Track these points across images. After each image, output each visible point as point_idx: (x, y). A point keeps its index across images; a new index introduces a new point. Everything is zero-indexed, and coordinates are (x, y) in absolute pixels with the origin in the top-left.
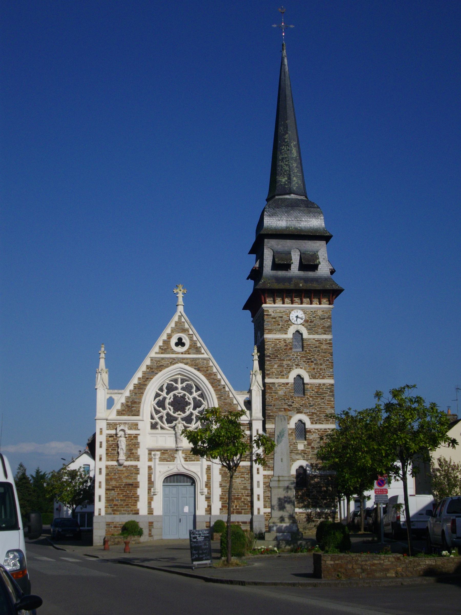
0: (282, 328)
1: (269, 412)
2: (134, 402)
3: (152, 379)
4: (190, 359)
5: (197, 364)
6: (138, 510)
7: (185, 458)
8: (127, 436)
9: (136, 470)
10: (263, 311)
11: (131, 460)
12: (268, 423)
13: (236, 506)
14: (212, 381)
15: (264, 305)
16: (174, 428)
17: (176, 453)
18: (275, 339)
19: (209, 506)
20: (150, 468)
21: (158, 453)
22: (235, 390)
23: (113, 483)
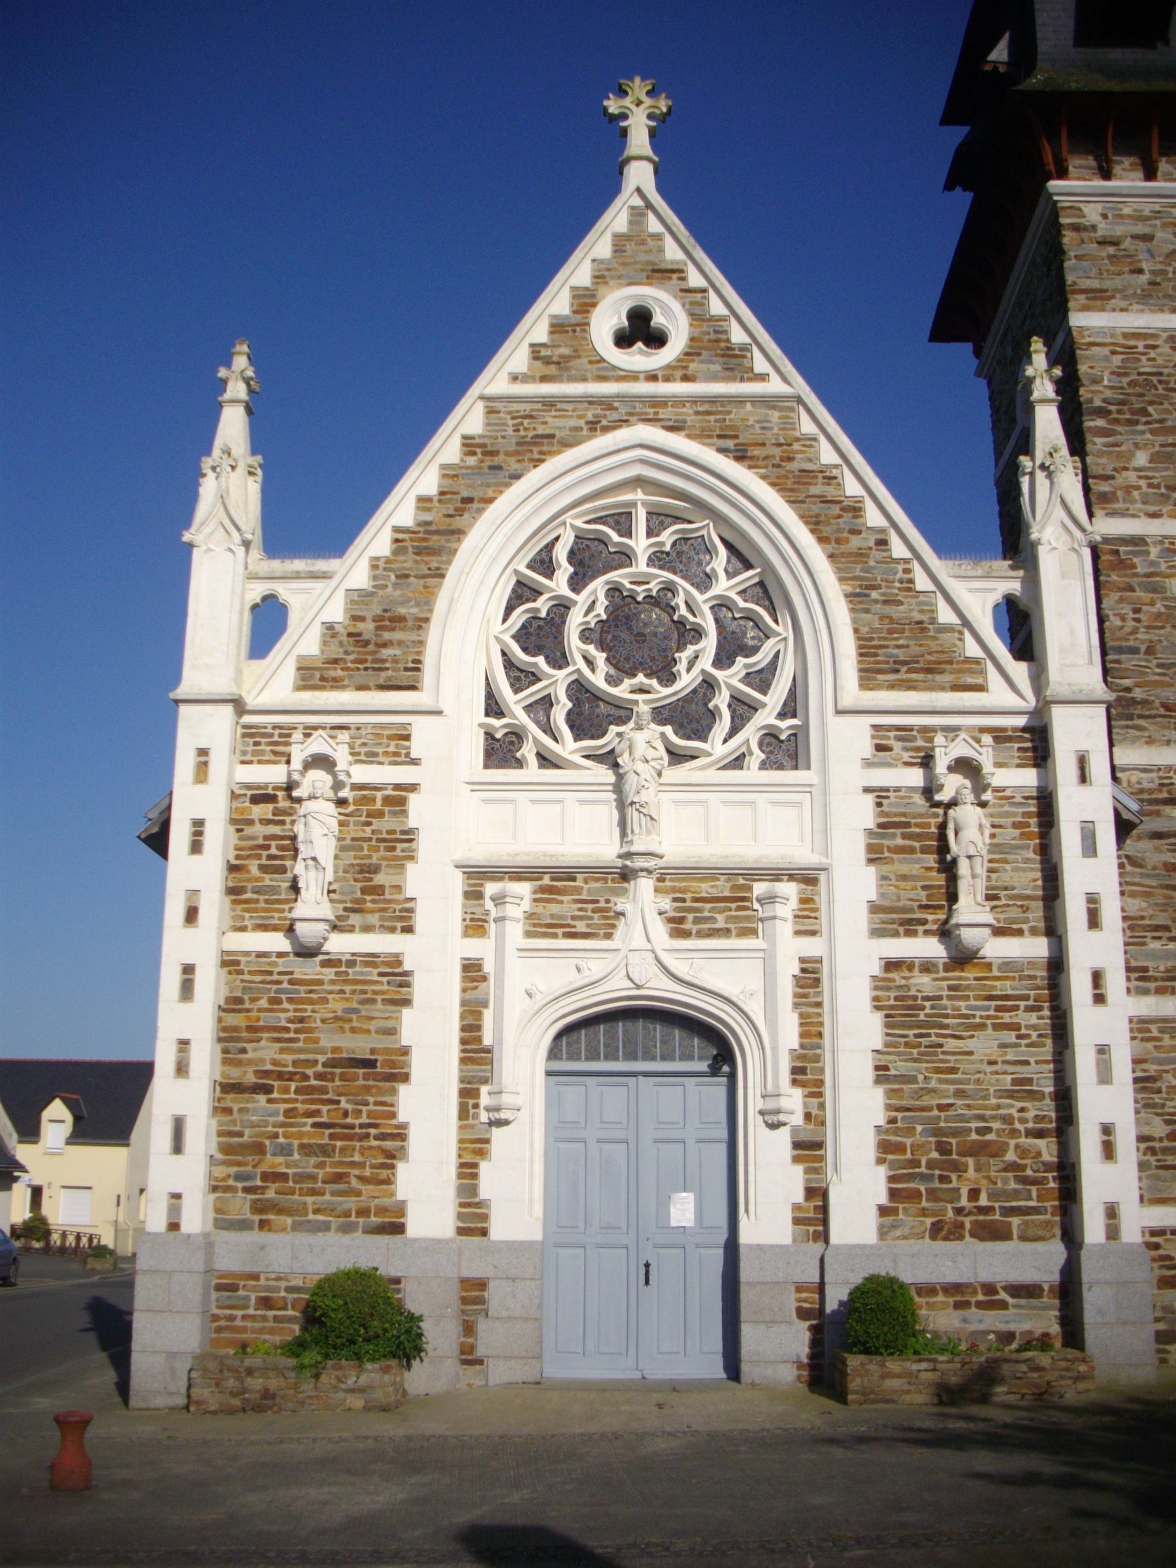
0: (1152, 283)
1: (1127, 682)
2: (390, 620)
3: (491, 501)
4: (695, 400)
5: (734, 427)
6: (400, 1209)
7: (671, 920)
8: (345, 793)
9: (396, 981)
10: (1055, 211)
11: (367, 929)
12: (1120, 742)
13: (974, 1194)
14: (816, 508)
15: (1054, 185)
16: (609, 759)
17: (624, 892)
18: (1126, 336)
19: (817, 1194)
20: (472, 971)
21: (524, 889)
22: (942, 551)
23: (265, 1052)
